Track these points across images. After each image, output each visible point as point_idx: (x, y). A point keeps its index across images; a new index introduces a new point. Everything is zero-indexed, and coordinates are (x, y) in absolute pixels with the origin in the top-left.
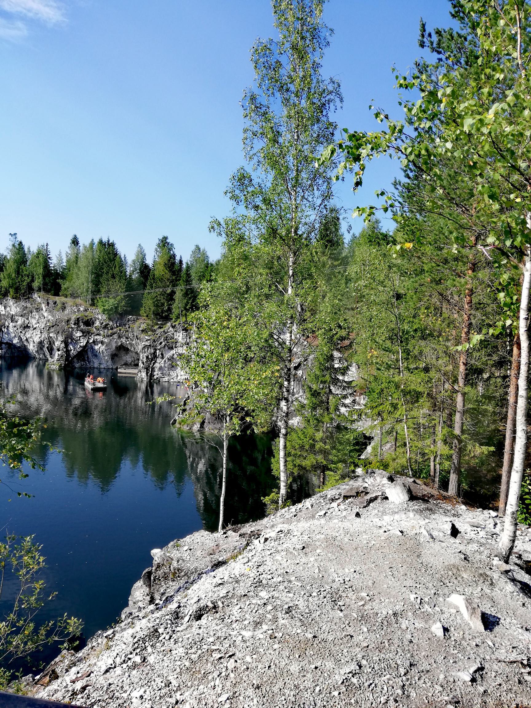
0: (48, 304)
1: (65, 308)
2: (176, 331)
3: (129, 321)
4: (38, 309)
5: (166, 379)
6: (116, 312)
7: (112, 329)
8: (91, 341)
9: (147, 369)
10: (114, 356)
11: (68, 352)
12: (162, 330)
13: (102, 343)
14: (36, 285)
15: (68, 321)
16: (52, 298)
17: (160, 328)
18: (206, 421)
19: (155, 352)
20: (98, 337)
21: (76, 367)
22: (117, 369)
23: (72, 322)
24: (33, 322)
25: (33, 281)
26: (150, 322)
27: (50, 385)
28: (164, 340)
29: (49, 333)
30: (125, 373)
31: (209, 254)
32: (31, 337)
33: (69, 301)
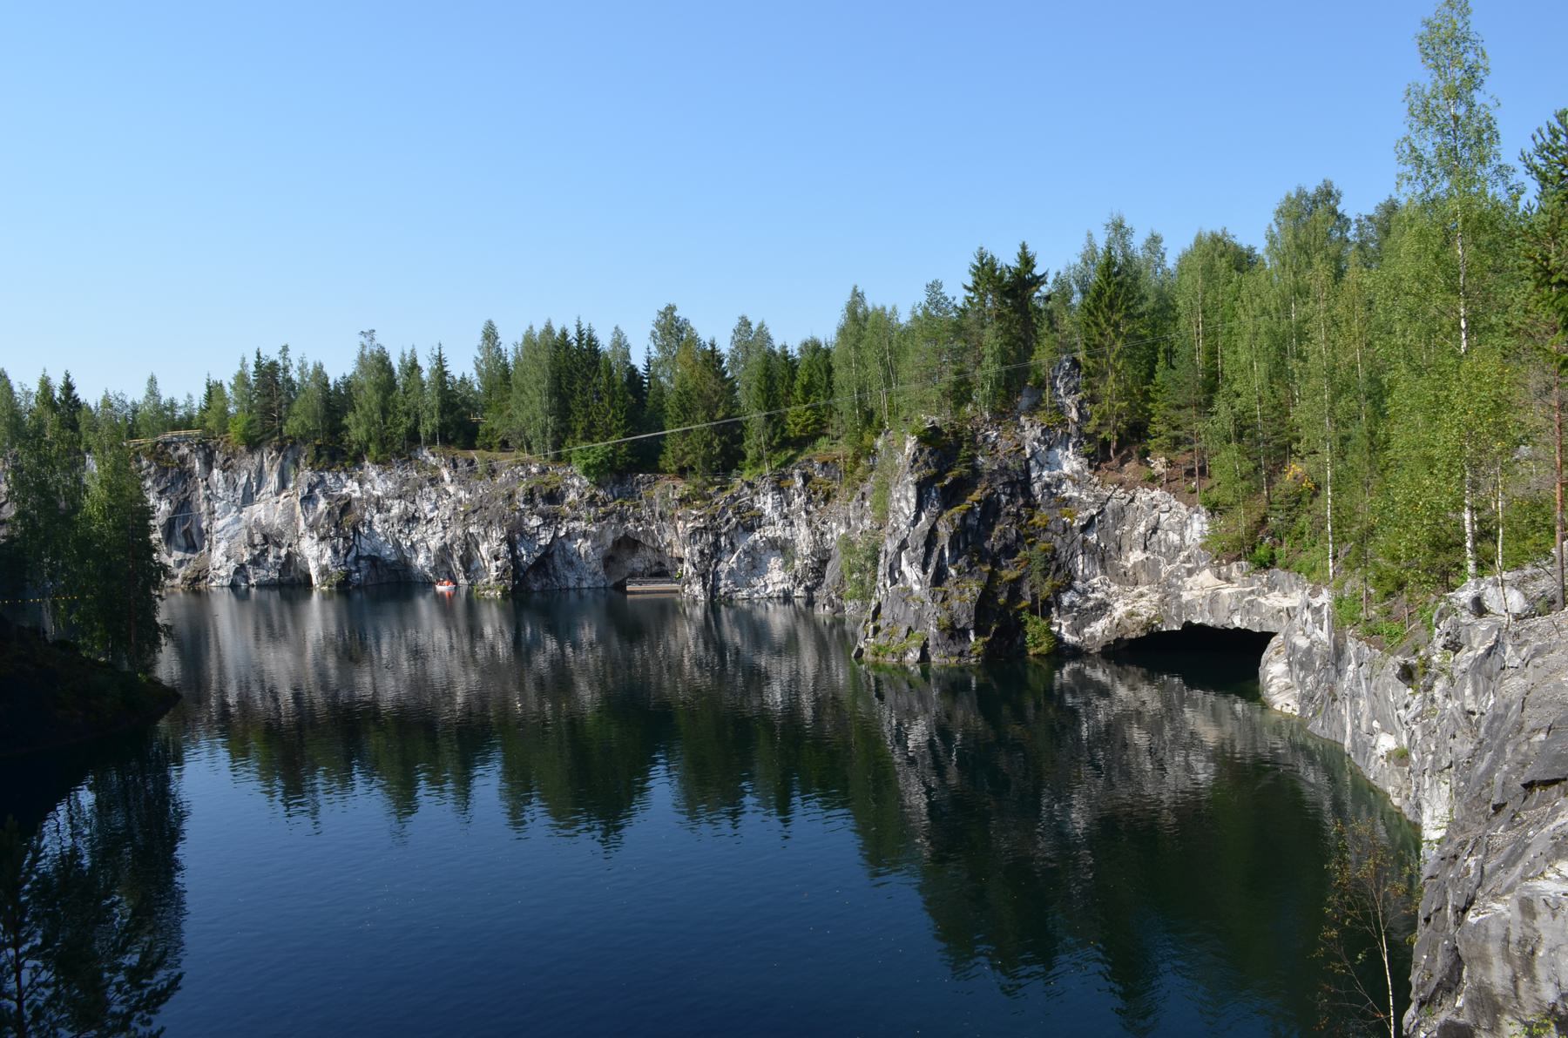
0: (455, 466)
1: (494, 471)
2: (757, 493)
3: (638, 483)
4: (435, 481)
5: (745, 593)
6: (612, 469)
7: (605, 504)
8: (562, 534)
9: (704, 576)
10: (609, 561)
11: (515, 559)
12: (727, 494)
13: (585, 535)
14: (426, 428)
15: (510, 496)
16: (461, 455)
17: (722, 490)
18: (931, 643)
19: (717, 540)
20: (576, 524)
21: (536, 589)
22: (620, 587)
23: (519, 497)
24: (427, 507)
25: (417, 423)
26: (699, 481)
27: (474, 632)
28: (734, 515)
29: (467, 526)
30: (643, 592)
31: (772, 333)
32: (423, 540)
33: (504, 459)
